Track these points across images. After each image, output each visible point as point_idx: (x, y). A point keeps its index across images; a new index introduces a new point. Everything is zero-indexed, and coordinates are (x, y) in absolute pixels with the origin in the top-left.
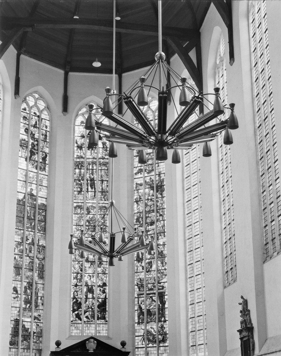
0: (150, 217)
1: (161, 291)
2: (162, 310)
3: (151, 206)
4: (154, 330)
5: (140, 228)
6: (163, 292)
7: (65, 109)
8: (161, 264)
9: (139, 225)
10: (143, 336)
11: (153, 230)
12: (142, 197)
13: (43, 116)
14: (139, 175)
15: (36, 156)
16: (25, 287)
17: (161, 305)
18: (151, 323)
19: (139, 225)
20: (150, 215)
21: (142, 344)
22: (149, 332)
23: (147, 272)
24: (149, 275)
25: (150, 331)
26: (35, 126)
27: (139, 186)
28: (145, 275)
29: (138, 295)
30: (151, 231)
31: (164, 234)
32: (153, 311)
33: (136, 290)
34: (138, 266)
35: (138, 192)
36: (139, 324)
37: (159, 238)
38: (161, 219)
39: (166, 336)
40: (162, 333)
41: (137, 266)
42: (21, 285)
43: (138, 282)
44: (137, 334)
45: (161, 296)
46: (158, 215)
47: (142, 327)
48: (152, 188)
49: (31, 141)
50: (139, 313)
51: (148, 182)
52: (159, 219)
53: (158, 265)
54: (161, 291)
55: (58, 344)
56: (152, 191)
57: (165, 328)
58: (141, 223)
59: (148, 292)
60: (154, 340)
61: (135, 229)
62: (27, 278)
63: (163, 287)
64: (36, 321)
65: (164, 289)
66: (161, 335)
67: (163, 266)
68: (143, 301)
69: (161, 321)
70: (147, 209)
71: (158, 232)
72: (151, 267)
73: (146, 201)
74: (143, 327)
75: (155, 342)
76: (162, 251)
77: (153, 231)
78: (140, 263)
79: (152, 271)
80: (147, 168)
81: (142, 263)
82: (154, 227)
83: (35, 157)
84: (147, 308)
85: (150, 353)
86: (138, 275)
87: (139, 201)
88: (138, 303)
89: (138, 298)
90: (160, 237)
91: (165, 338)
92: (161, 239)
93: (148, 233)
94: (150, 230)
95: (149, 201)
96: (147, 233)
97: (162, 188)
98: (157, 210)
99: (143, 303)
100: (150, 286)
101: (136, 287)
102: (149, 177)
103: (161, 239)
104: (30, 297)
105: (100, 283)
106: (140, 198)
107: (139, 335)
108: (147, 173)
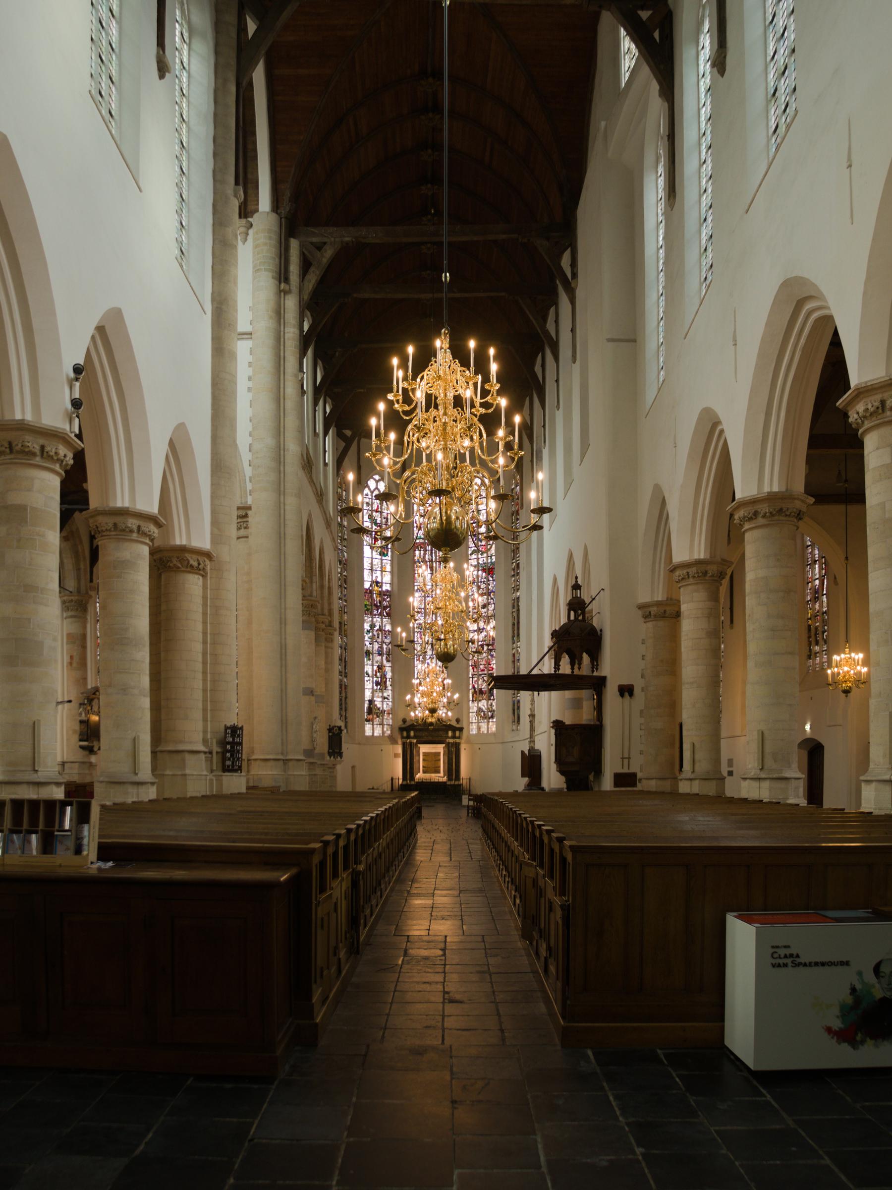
1: (491, 672)
16: (376, 672)
29: (472, 675)
42: (373, 669)
54: (491, 672)
59: (480, 673)
62: (377, 662)
63: (493, 669)
64: (386, 700)
65: (494, 670)
66: (491, 712)
68: (476, 681)
69: (491, 700)
74: (476, 705)
89: (472, 678)
100: (482, 667)
101: (471, 668)
104: (380, 679)
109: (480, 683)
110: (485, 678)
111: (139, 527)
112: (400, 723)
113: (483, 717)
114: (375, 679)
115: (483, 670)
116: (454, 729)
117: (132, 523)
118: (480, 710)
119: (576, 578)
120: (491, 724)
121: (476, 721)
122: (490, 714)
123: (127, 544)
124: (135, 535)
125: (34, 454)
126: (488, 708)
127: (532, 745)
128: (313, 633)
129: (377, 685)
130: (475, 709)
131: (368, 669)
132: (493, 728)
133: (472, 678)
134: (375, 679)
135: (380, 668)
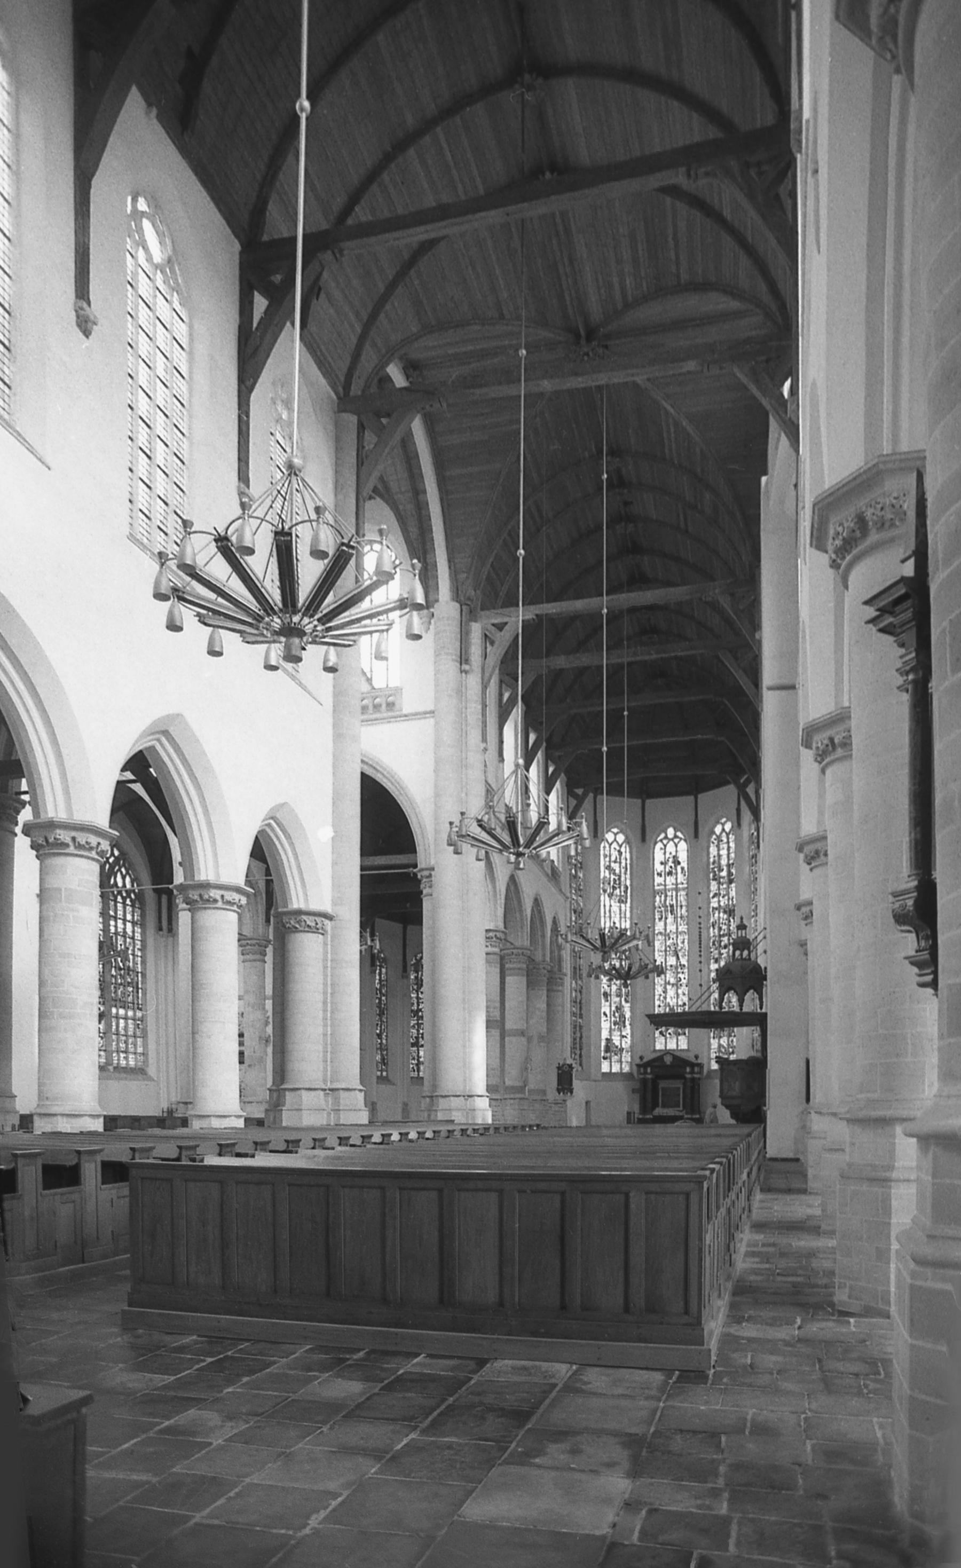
7: (643, 839)
13: (623, 850)
14: (716, 899)
15: (618, 890)
26: (615, 862)
48: (725, 912)
49: (613, 877)
55: (641, 1058)
56: (725, 916)
83: (617, 892)
105: (680, 1003)
111: (222, 896)
112: (638, 1061)
114: (613, 1019)
116: (692, 1065)
117: (215, 894)
118: (720, 1046)
119: (742, 918)
123: (209, 912)
124: (220, 904)
125: (67, 845)
126: (728, 1045)
128: (525, 979)
129: (615, 1025)
131: (605, 1008)
134: (613, 1019)
135: (620, 1008)
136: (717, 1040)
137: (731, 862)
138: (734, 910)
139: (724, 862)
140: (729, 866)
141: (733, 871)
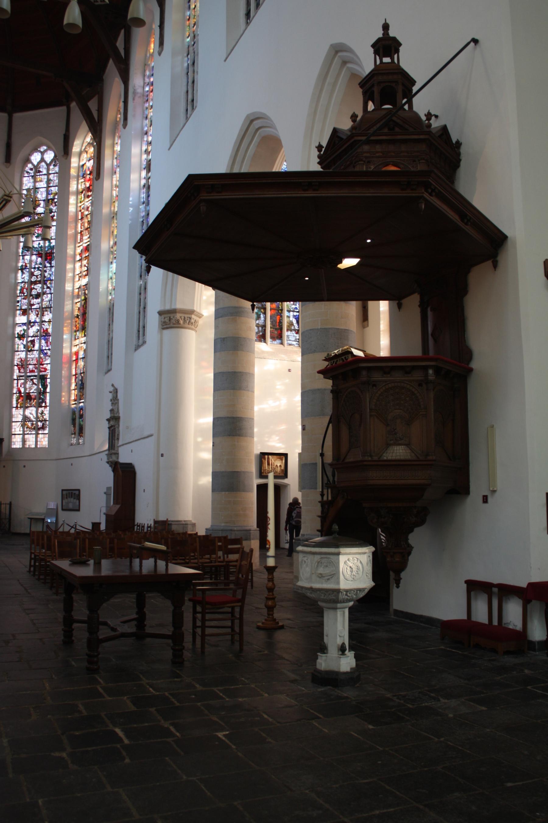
0: (36, 289)
1: (43, 373)
2: (42, 393)
3: (38, 277)
4: (33, 416)
5: (24, 300)
6: (45, 375)
8: (45, 344)
9: (22, 297)
10: (21, 422)
11: (39, 304)
12: (28, 265)
17: (42, 389)
18: (30, 408)
19: (22, 297)
20: (35, 287)
21: (20, 431)
22: (28, 418)
23: (29, 351)
24: (31, 354)
25: (29, 417)
27: (26, 252)
28: (27, 355)
29: (18, 376)
30: (36, 305)
31: (51, 310)
32: (33, 395)
33: (15, 371)
34: (19, 344)
35: (23, 259)
36: (18, 409)
37: (45, 314)
38: (48, 292)
39: (46, 423)
40: (42, 419)
41: (18, 344)
43: (18, 363)
44: (14, 420)
45: (43, 379)
46: (45, 287)
47: (20, 412)
48: (39, 255)
50: (17, 397)
51: (36, 248)
52: (46, 292)
53: (42, 344)
56: (39, 260)
57: (45, 414)
58: (26, 294)
59: (28, 374)
60: (33, 427)
61: (18, 302)
63: (46, 370)
65: (47, 371)
66: (41, 421)
67: (47, 346)
68: (23, 384)
69: (42, 407)
70: (33, 279)
71: (44, 307)
72: (34, 346)
73: (33, 270)
74: (22, 413)
75: (34, 429)
76: (47, 329)
77: (38, 305)
78: (21, 341)
79: (35, 350)
80: (36, 231)
81: (23, 340)
82: (39, 300)
84: (27, 391)
85: (27, 441)
86: (19, 355)
87: (24, 269)
88: (18, 386)
89: (18, 380)
90: (46, 313)
91: (44, 425)
92: (47, 316)
93: (33, 307)
94: (35, 303)
95: (35, 270)
96: (31, 307)
97: (52, 256)
98: (44, 281)
99: (22, 386)
100: (31, 367)
101: (16, 368)
102: (38, 243)
103: (47, 316)
106: (26, 266)
107: (17, 421)
108: (36, 237)
109: (28, 386)
110: (35, 381)
113: (29, 428)
115: (32, 371)
118: (25, 419)
120: (40, 436)
121: (21, 432)
122: (40, 424)
126: (37, 417)
127: (114, 458)
130: (20, 418)
132: (44, 441)
133: (18, 380)
136: (21, 411)
137: (51, 197)
138: (51, 253)
139: (41, 195)
140: (48, 201)
141: (54, 209)
